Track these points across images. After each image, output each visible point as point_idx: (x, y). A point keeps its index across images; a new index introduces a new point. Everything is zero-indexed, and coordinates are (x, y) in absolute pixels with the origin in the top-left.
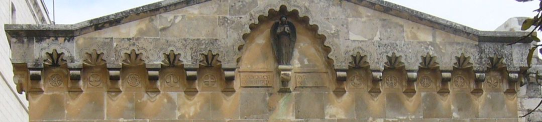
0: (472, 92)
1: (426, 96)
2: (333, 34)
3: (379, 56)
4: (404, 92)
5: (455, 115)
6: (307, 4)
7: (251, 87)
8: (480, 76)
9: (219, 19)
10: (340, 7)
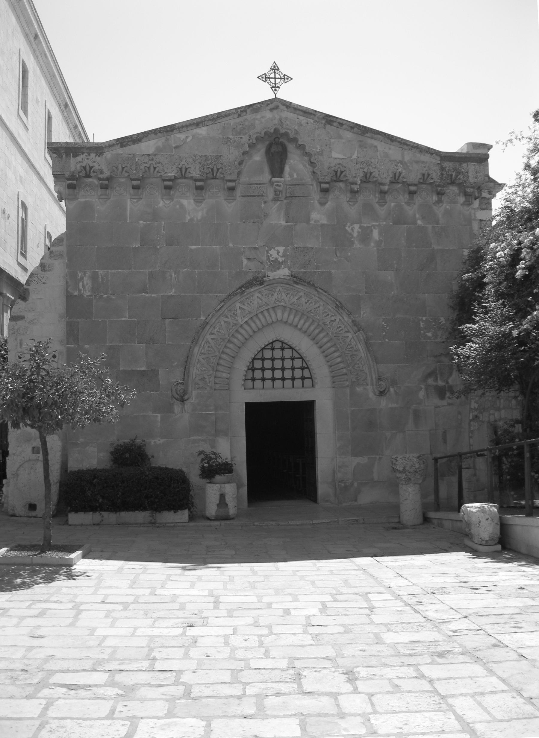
0: (434, 204)
2: (318, 152)
4: (377, 202)
5: (419, 222)
6: (296, 128)
7: (249, 196)
8: (441, 189)
9: (223, 137)
10: (324, 130)
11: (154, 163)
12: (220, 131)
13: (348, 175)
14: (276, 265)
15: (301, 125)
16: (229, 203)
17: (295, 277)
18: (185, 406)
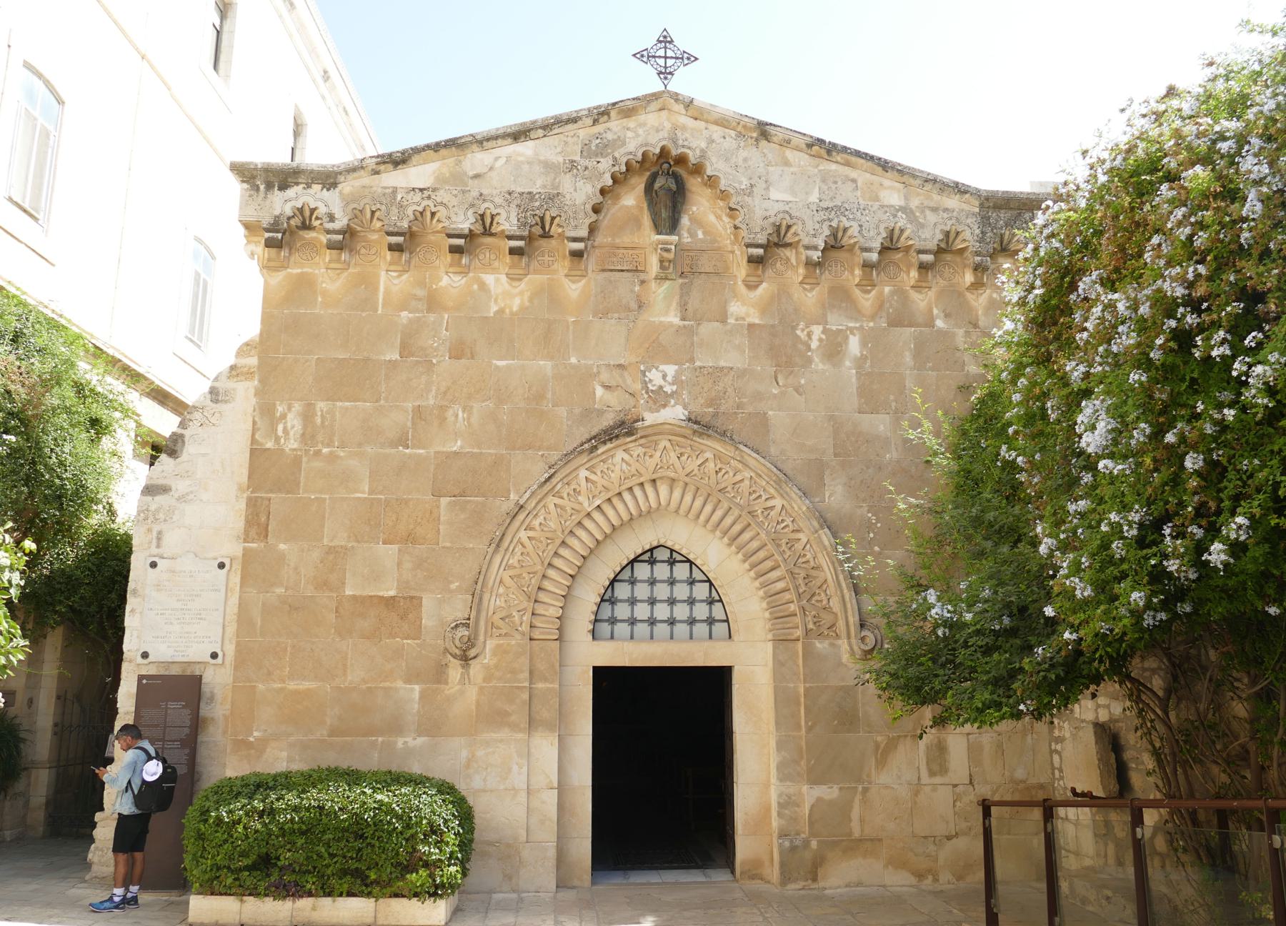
1: (893, 293)
3: (817, 226)
6: (703, 145)
7: (611, 270)
9: (565, 163)
11: (432, 205)
12: (559, 150)
13: (801, 233)
14: (659, 399)
15: (713, 141)
16: (573, 282)
17: (696, 422)
18: (472, 672)
